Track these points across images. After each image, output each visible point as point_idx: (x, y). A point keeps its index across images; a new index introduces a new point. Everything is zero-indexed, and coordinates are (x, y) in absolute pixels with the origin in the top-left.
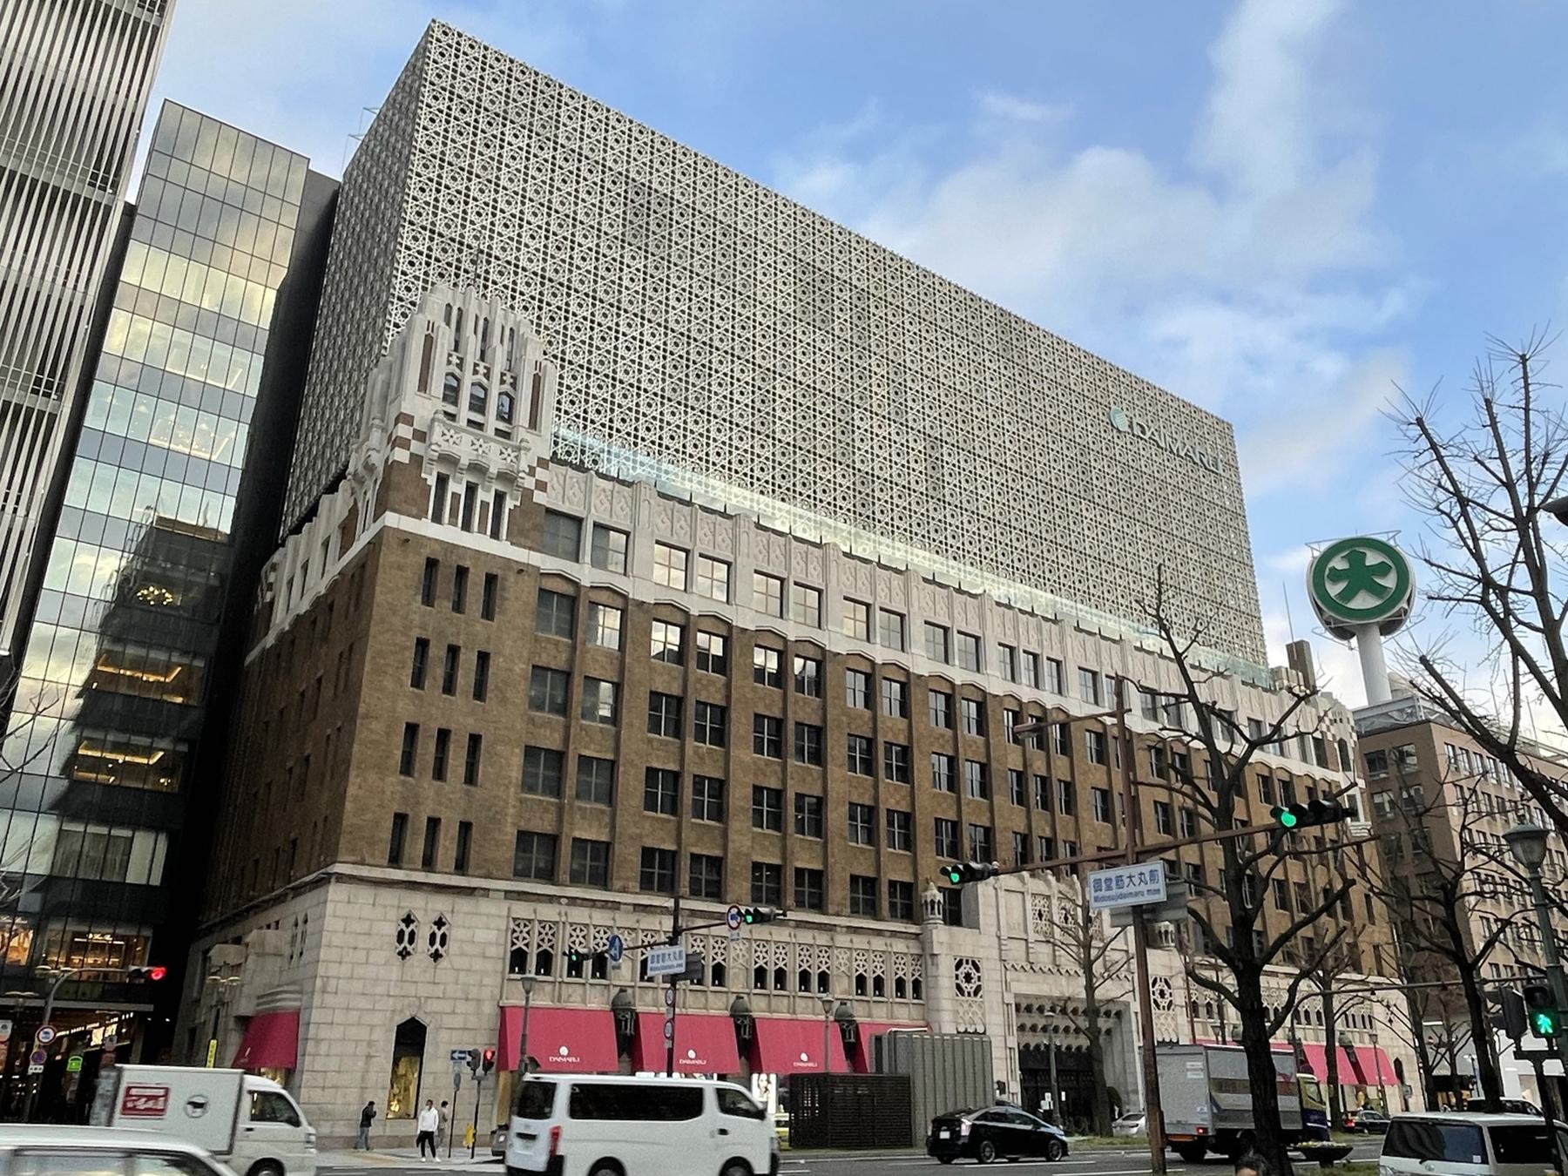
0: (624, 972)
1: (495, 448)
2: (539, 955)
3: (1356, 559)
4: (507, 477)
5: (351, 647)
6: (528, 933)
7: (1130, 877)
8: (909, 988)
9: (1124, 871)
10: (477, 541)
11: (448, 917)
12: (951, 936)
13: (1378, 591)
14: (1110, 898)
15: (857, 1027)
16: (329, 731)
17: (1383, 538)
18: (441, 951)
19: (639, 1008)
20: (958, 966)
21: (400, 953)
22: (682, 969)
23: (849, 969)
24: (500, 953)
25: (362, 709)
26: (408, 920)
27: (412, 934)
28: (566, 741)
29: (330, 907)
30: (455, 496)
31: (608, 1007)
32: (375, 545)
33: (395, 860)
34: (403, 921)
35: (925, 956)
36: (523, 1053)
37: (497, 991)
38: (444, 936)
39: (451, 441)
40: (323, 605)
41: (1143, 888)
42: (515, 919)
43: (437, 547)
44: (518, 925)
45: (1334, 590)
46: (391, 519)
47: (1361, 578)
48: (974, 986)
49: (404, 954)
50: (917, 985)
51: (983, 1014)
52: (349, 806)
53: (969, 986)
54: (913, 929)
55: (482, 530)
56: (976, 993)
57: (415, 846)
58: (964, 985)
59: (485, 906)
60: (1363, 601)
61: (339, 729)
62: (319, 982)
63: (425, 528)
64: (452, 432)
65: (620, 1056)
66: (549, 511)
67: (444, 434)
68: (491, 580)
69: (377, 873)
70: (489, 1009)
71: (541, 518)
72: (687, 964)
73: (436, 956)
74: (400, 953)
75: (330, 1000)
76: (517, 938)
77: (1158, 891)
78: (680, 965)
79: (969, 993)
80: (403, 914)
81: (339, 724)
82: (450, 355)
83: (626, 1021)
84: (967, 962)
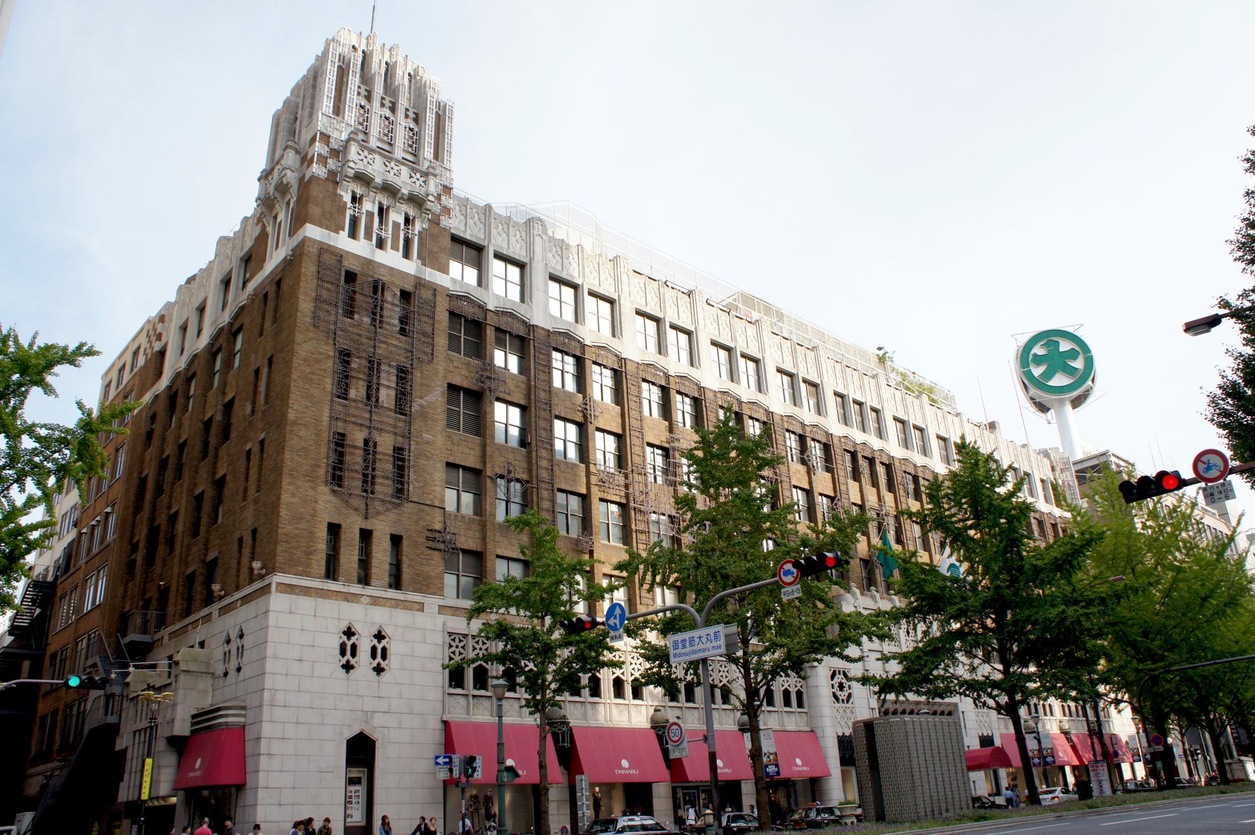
5: (270, 360)
6: (463, 647)
10: (391, 259)
11: (388, 631)
13: (1071, 371)
16: (248, 447)
17: (1070, 330)
19: (573, 722)
25: (291, 415)
26: (349, 633)
27: (354, 647)
28: (484, 458)
29: (272, 619)
30: (370, 215)
32: (291, 263)
37: (439, 706)
38: (384, 650)
42: (450, 634)
43: (355, 262)
44: (454, 640)
45: (1037, 371)
46: (312, 231)
48: (847, 694)
49: (348, 667)
50: (799, 694)
52: (283, 512)
53: (843, 694)
55: (395, 247)
56: (848, 702)
57: (349, 557)
58: (838, 693)
62: (267, 695)
63: (342, 241)
66: (456, 239)
71: (447, 242)
73: (379, 670)
75: (279, 713)
76: (454, 653)
78: (719, 647)
81: (262, 436)
82: (359, 87)
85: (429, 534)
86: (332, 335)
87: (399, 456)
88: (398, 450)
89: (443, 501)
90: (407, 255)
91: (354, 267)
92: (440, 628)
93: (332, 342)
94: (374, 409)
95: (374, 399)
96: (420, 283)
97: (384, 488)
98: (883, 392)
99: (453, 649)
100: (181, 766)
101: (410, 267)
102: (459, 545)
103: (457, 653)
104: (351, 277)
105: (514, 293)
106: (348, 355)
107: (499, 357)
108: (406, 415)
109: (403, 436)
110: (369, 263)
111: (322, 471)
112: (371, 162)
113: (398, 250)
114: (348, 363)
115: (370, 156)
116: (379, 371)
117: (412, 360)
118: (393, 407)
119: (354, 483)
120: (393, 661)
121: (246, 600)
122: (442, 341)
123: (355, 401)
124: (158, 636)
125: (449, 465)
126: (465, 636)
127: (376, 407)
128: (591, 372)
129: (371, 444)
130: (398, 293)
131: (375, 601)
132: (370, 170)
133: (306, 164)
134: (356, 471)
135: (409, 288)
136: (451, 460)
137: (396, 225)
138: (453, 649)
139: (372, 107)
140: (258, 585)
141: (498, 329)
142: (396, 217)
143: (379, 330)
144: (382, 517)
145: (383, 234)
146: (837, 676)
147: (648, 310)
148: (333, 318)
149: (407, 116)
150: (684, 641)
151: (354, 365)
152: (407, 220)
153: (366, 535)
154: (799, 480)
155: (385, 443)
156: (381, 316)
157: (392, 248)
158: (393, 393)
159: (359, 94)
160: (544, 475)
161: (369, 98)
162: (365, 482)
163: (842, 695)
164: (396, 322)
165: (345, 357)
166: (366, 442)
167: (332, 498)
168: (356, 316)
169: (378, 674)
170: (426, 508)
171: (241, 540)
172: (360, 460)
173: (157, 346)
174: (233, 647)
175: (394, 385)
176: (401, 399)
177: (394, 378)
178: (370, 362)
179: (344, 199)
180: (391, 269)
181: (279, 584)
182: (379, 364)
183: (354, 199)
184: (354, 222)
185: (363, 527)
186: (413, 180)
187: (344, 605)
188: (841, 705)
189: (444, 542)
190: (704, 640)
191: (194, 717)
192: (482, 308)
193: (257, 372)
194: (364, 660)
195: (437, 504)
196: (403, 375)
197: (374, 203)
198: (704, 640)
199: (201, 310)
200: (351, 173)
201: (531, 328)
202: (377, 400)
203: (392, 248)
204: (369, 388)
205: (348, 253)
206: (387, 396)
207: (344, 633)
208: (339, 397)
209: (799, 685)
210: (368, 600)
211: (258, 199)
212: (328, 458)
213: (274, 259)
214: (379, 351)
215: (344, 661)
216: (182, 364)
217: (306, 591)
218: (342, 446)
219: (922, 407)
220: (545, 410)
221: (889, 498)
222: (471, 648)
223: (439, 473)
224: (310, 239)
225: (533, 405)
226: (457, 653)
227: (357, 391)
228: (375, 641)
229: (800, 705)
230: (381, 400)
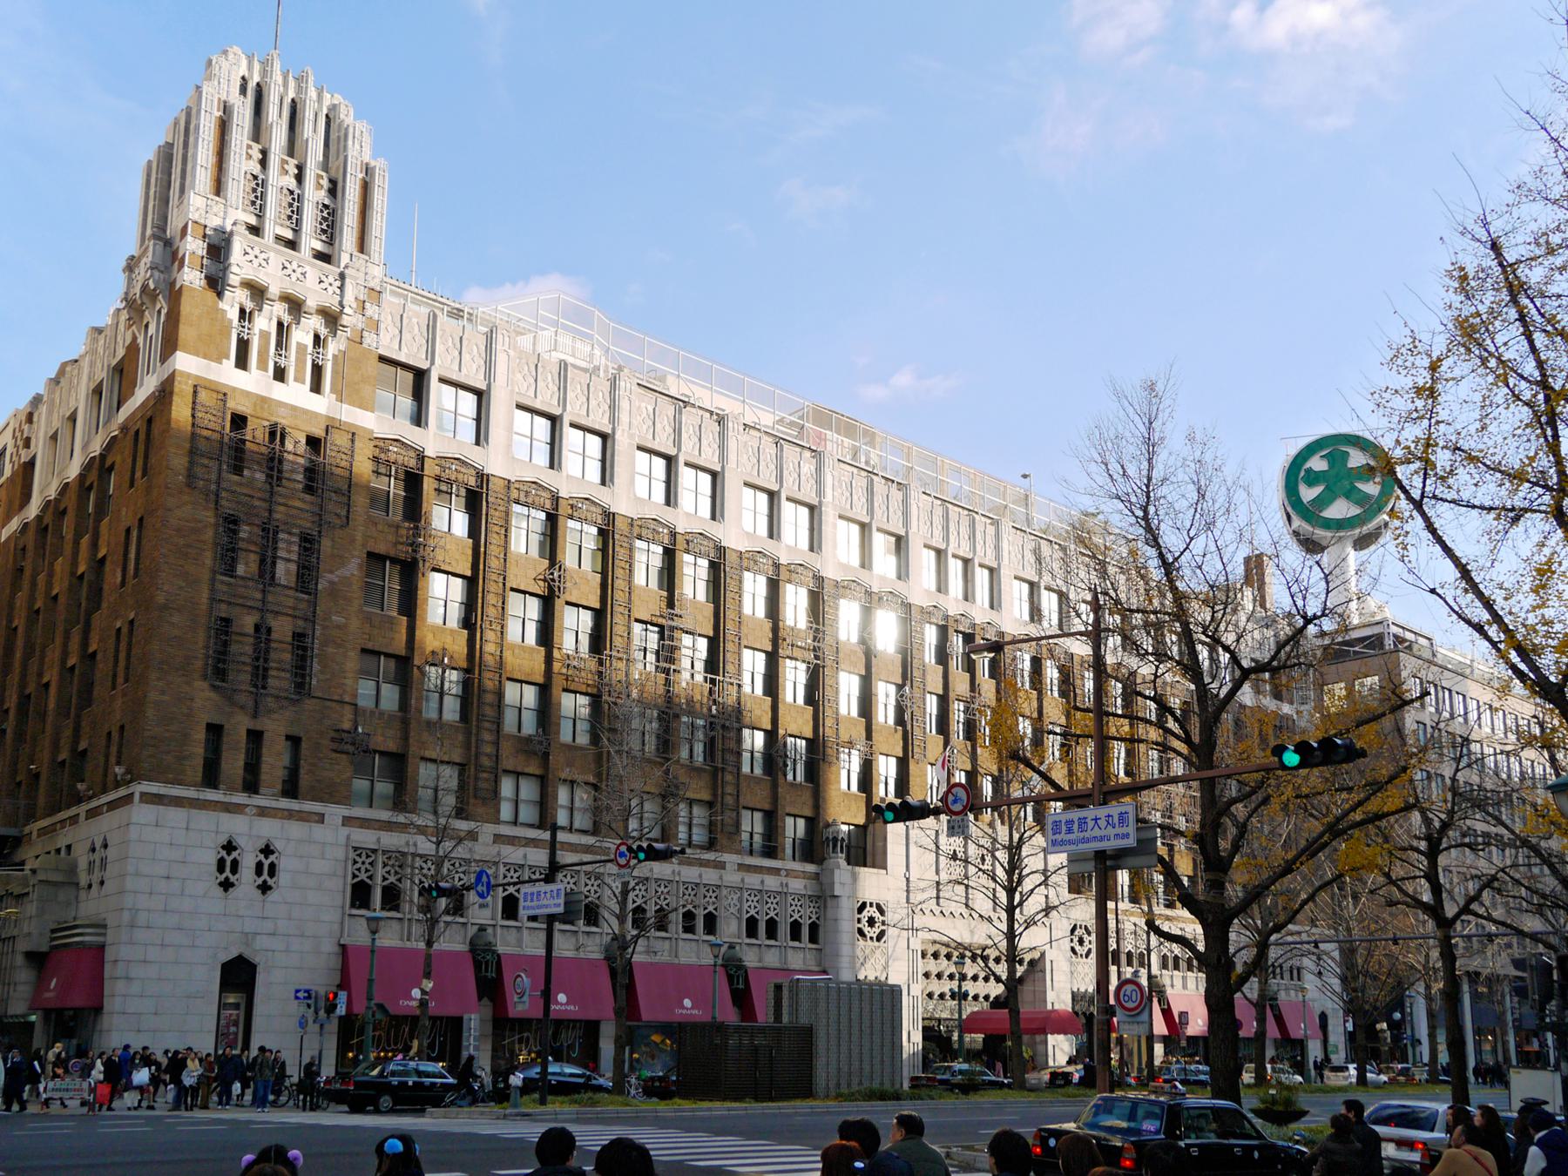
1: (315, 269)
3: (1337, 459)
4: (332, 319)
7: (1096, 819)
9: (1091, 812)
10: (295, 393)
11: (278, 845)
16: (118, 625)
18: (270, 882)
19: (501, 949)
24: (337, 891)
30: (265, 335)
31: (464, 948)
34: (223, 847)
36: (370, 999)
37: (336, 927)
38: (272, 867)
40: (99, 468)
41: (1111, 831)
42: (355, 849)
44: (360, 855)
47: (1339, 481)
55: (299, 379)
57: (233, 763)
59: (318, 831)
60: (1339, 509)
61: (132, 622)
65: (480, 999)
66: (383, 359)
69: (190, 793)
73: (265, 888)
74: (221, 884)
76: (359, 870)
77: (1127, 836)
80: (223, 840)
81: (132, 616)
83: (487, 963)
85: (333, 734)
88: (299, 636)
90: (316, 387)
91: (243, 408)
92: (342, 840)
93: (213, 506)
94: (268, 588)
95: (268, 576)
97: (280, 681)
100: (40, 984)
101: (321, 405)
103: (363, 870)
106: (235, 522)
108: (310, 594)
110: (264, 401)
111: (199, 664)
113: (303, 383)
114: (235, 532)
116: (275, 541)
117: (320, 525)
118: (293, 585)
119: (242, 678)
120: (283, 878)
123: (243, 578)
125: (364, 651)
126: (374, 851)
127: (270, 585)
129: (263, 630)
130: (303, 441)
131: (263, 812)
134: (244, 663)
135: (319, 432)
137: (301, 348)
140: (122, 792)
142: (301, 336)
143: (277, 489)
144: (275, 716)
145: (282, 362)
148: (214, 477)
151: (242, 535)
152: (317, 339)
153: (255, 737)
155: (282, 628)
156: (280, 471)
157: (296, 380)
158: (293, 567)
162: (255, 675)
164: (300, 477)
165: (231, 523)
166: (257, 628)
167: (213, 695)
168: (246, 472)
171: (109, 734)
172: (249, 649)
174: (97, 856)
175: (295, 557)
177: (296, 548)
178: (263, 530)
180: (294, 408)
182: (276, 533)
186: (323, 285)
187: (224, 817)
189: (353, 744)
193: (128, 531)
196: (308, 543)
197: (271, 319)
202: (273, 577)
203: (296, 380)
204: (262, 561)
206: (285, 571)
207: (223, 847)
208: (222, 574)
212: (207, 647)
214: (276, 516)
217: (178, 802)
218: (227, 633)
222: (380, 865)
226: (363, 870)
228: (262, 857)
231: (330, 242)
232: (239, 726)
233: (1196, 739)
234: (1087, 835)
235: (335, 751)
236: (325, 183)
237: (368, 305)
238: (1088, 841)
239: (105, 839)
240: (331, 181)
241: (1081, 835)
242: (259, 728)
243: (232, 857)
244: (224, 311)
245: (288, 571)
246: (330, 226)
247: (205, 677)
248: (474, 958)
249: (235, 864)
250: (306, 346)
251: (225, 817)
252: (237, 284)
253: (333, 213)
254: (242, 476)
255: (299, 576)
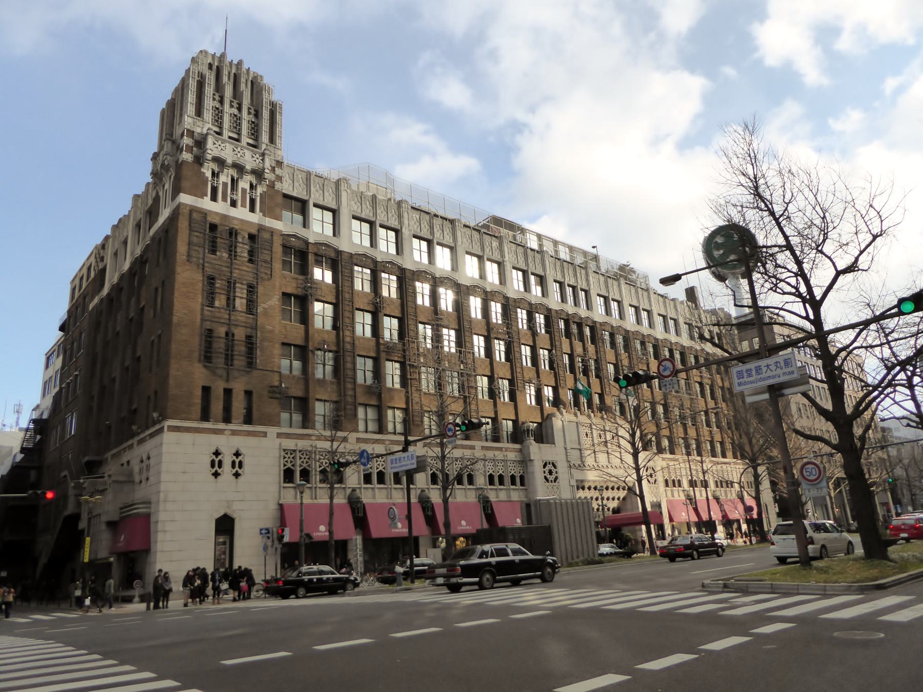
0: (353, 477)
2: (301, 472)
4: (259, 174)
8: (518, 480)
10: (241, 213)
11: (242, 450)
12: (540, 448)
14: (751, 382)
15: (491, 504)
16: (153, 338)
18: (240, 471)
19: (365, 501)
20: (545, 466)
21: (213, 474)
22: (415, 466)
23: (485, 472)
25: (175, 320)
26: (217, 453)
29: (165, 448)
30: (225, 185)
33: (205, 417)
35: (525, 461)
37: (277, 495)
38: (240, 463)
39: (220, 148)
40: (140, 263)
41: (779, 371)
42: (284, 450)
45: (717, 253)
46: (185, 199)
48: (554, 477)
49: (216, 475)
50: (522, 478)
51: (560, 493)
52: (171, 382)
54: (517, 446)
55: (243, 205)
56: (555, 481)
57: (217, 407)
58: (548, 476)
62: (162, 495)
63: (206, 203)
64: (220, 142)
66: (286, 196)
67: (214, 144)
68: (252, 237)
70: (273, 506)
71: (280, 199)
72: (418, 462)
73: (237, 475)
74: (213, 474)
76: (287, 461)
78: (413, 464)
79: (551, 481)
81: (160, 332)
83: (358, 508)
84: (549, 464)
86: (201, 266)
87: (250, 342)
88: (249, 337)
89: (280, 367)
90: (252, 210)
91: (216, 220)
92: (277, 446)
93: (201, 271)
94: (232, 313)
95: (231, 306)
96: (261, 228)
97: (240, 362)
98: (591, 278)
99: (286, 460)
101: (255, 218)
102: (290, 394)
103: (289, 462)
104: (213, 227)
105: (329, 230)
106: (213, 279)
107: (317, 273)
109: (252, 329)
110: (225, 217)
111: (197, 354)
112: (224, 149)
113: (245, 207)
114: (213, 284)
115: (223, 145)
116: (234, 288)
117: (257, 279)
118: (245, 310)
119: (219, 361)
121: (152, 436)
122: (277, 266)
123: (218, 308)
124: (105, 456)
125: (283, 344)
126: (294, 451)
127: (233, 311)
128: (381, 278)
129: (230, 335)
130: (247, 236)
131: (234, 433)
132: (223, 155)
133: (179, 151)
134: (221, 353)
135: (254, 231)
136: (286, 341)
137: (244, 190)
138: (286, 460)
139: (224, 108)
140: (157, 427)
141: (316, 254)
142: (244, 184)
143: (234, 261)
145: (235, 197)
146: (548, 465)
147: (422, 235)
148: (201, 256)
149: (249, 113)
150: (396, 459)
151: (217, 285)
152: (252, 186)
153: (228, 392)
154: (526, 340)
155: (240, 333)
156: (236, 252)
157: (242, 206)
158: (244, 301)
159: (214, 99)
160: (348, 347)
161: (221, 102)
162: (226, 359)
163: (551, 478)
164: (246, 255)
165: (211, 280)
166: (227, 334)
167: (205, 371)
168: (218, 253)
169: (237, 478)
170: (269, 373)
171: (149, 398)
172: (223, 346)
173: (101, 266)
174: (144, 465)
175: (245, 296)
176: (250, 305)
177: (245, 291)
178: (228, 282)
179: (206, 175)
180: (242, 221)
181: (169, 427)
182: (235, 284)
183: (213, 174)
184: (214, 190)
185: (226, 387)
188: (550, 484)
189: (280, 393)
190: (406, 459)
191: (121, 509)
192: (307, 243)
193: (156, 289)
194: (227, 468)
195: (276, 369)
197: (228, 176)
198: (406, 459)
199: (125, 243)
200: (209, 157)
201: (339, 252)
202: (234, 307)
203: (242, 206)
204: (228, 299)
205: (211, 212)
206: (240, 303)
208: (207, 306)
209: (521, 472)
210: (229, 432)
211: (152, 173)
212: (200, 345)
213: (164, 214)
214: (235, 275)
215: (213, 471)
216: (115, 280)
218: (211, 337)
219: (619, 285)
220: (349, 305)
221: (591, 348)
222: (298, 458)
223: (277, 350)
224: (183, 204)
225: (341, 302)
226: (289, 462)
227: (220, 301)
228: (234, 458)
229: (522, 484)
230: (236, 306)
231: (256, 139)
232: (219, 388)
233: (812, 317)
234: (762, 376)
235: (271, 398)
236: (252, 111)
237: (276, 169)
238: (764, 379)
239: (149, 454)
240: (255, 110)
241: (759, 377)
242: (230, 387)
243: (218, 459)
244: (204, 173)
245: (241, 303)
246: (255, 132)
247: (200, 361)
248: (351, 507)
249: (220, 463)
250: (246, 190)
251: (214, 437)
252: (210, 159)
253: (257, 125)
254: (216, 255)
255: (248, 306)
